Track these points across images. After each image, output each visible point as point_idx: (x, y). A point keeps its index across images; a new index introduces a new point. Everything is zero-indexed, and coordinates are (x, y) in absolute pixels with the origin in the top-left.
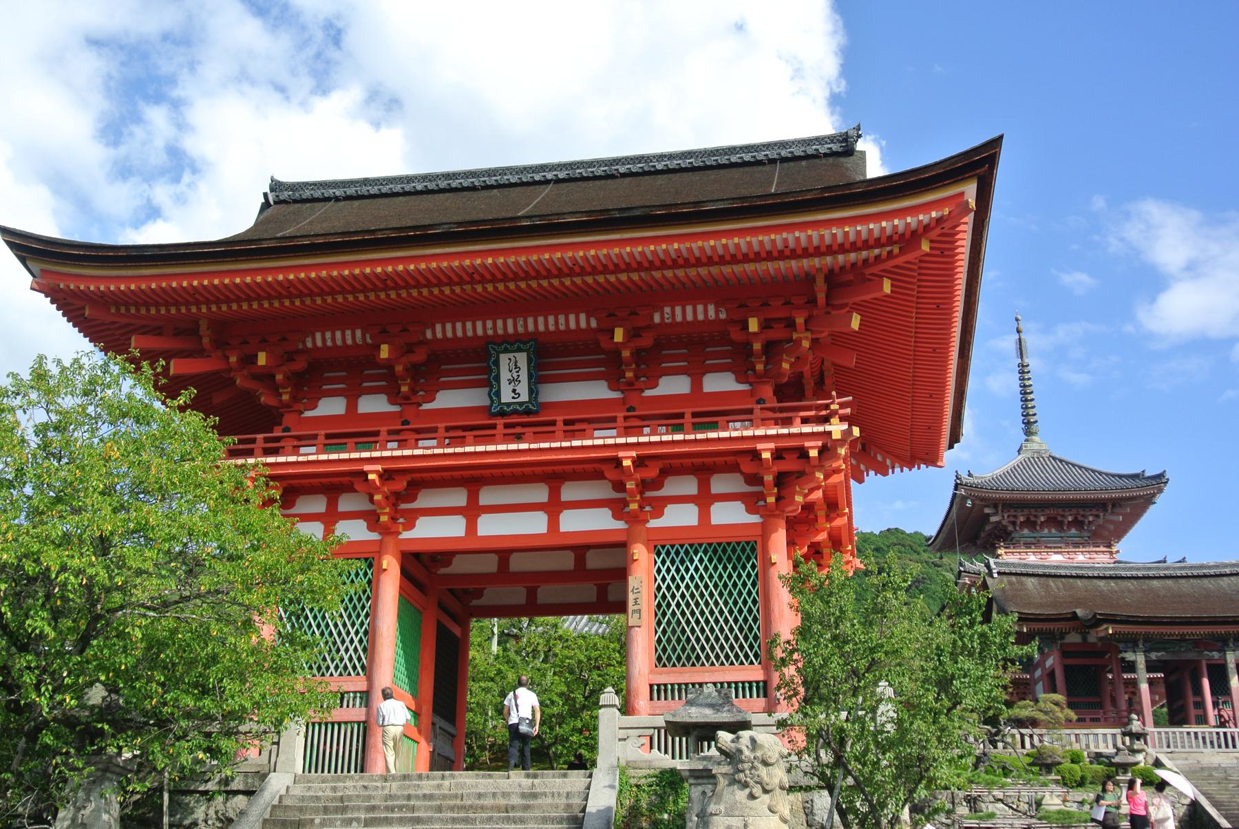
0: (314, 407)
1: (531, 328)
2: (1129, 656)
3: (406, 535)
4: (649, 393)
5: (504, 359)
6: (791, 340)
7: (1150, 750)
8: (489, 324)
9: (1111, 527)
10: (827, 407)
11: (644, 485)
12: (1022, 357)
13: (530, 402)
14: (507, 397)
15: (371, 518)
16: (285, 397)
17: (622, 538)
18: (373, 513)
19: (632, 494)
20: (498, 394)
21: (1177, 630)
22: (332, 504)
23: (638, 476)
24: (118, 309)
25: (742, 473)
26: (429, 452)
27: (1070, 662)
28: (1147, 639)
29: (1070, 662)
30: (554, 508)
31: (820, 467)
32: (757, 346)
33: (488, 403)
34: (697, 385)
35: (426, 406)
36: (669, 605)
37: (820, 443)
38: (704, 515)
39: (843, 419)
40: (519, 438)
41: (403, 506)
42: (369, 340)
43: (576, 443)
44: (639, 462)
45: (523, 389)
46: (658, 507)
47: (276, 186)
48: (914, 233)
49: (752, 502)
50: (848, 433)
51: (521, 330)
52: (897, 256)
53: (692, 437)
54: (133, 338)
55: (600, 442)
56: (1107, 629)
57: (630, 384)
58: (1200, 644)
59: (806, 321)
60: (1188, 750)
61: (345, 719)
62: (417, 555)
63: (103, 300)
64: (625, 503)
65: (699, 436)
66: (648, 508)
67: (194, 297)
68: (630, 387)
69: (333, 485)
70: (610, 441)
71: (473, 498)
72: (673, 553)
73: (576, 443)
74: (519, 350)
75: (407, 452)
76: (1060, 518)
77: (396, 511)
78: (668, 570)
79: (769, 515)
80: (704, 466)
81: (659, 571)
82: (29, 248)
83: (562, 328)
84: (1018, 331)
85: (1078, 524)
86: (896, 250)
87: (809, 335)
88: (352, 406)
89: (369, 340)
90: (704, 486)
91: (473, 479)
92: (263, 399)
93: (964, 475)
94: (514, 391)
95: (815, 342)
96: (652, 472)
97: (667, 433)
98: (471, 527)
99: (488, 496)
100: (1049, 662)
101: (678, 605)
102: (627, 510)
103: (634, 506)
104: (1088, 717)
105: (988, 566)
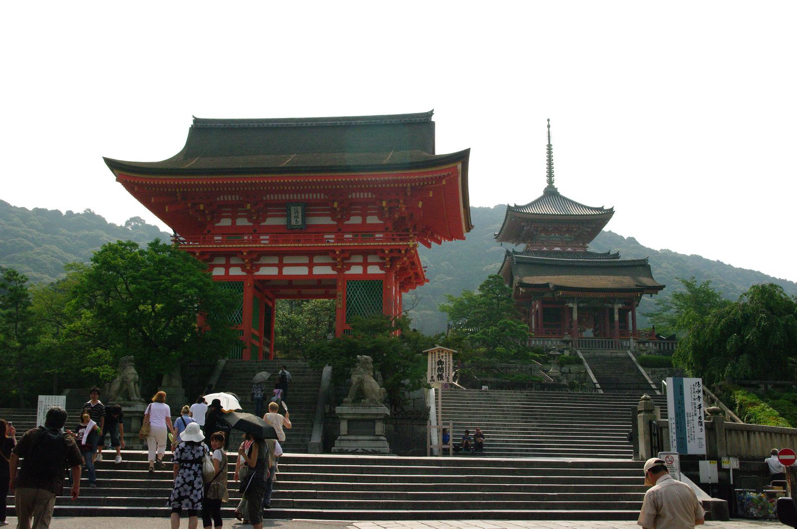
0: (219, 222)
2: (570, 305)
3: (256, 273)
4: (346, 222)
5: (293, 208)
6: (398, 207)
9: (586, 233)
10: (408, 235)
12: (549, 142)
14: (293, 222)
16: (209, 219)
19: (339, 262)
20: (290, 221)
21: (591, 295)
22: (228, 261)
23: (341, 256)
24: (148, 188)
30: (311, 265)
31: (405, 256)
32: (386, 209)
33: (286, 223)
34: (364, 220)
36: (351, 302)
37: (405, 248)
38: (365, 270)
40: (299, 241)
43: (320, 245)
44: (342, 252)
45: (300, 220)
47: (196, 121)
52: (434, 184)
56: (560, 293)
60: (591, 348)
62: (259, 281)
67: (178, 186)
72: (353, 283)
74: (299, 205)
75: (258, 245)
76: (560, 229)
77: (252, 264)
79: (388, 271)
80: (365, 253)
81: (348, 290)
84: (549, 126)
85: (569, 231)
86: (434, 182)
87: (404, 206)
88: (234, 223)
89: (241, 199)
90: (365, 259)
91: (281, 254)
92: (199, 219)
93: (513, 206)
95: (407, 208)
98: (280, 271)
99: (286, 260)
100: (537, 306)
101: (355, 302)
103: (340, 267)
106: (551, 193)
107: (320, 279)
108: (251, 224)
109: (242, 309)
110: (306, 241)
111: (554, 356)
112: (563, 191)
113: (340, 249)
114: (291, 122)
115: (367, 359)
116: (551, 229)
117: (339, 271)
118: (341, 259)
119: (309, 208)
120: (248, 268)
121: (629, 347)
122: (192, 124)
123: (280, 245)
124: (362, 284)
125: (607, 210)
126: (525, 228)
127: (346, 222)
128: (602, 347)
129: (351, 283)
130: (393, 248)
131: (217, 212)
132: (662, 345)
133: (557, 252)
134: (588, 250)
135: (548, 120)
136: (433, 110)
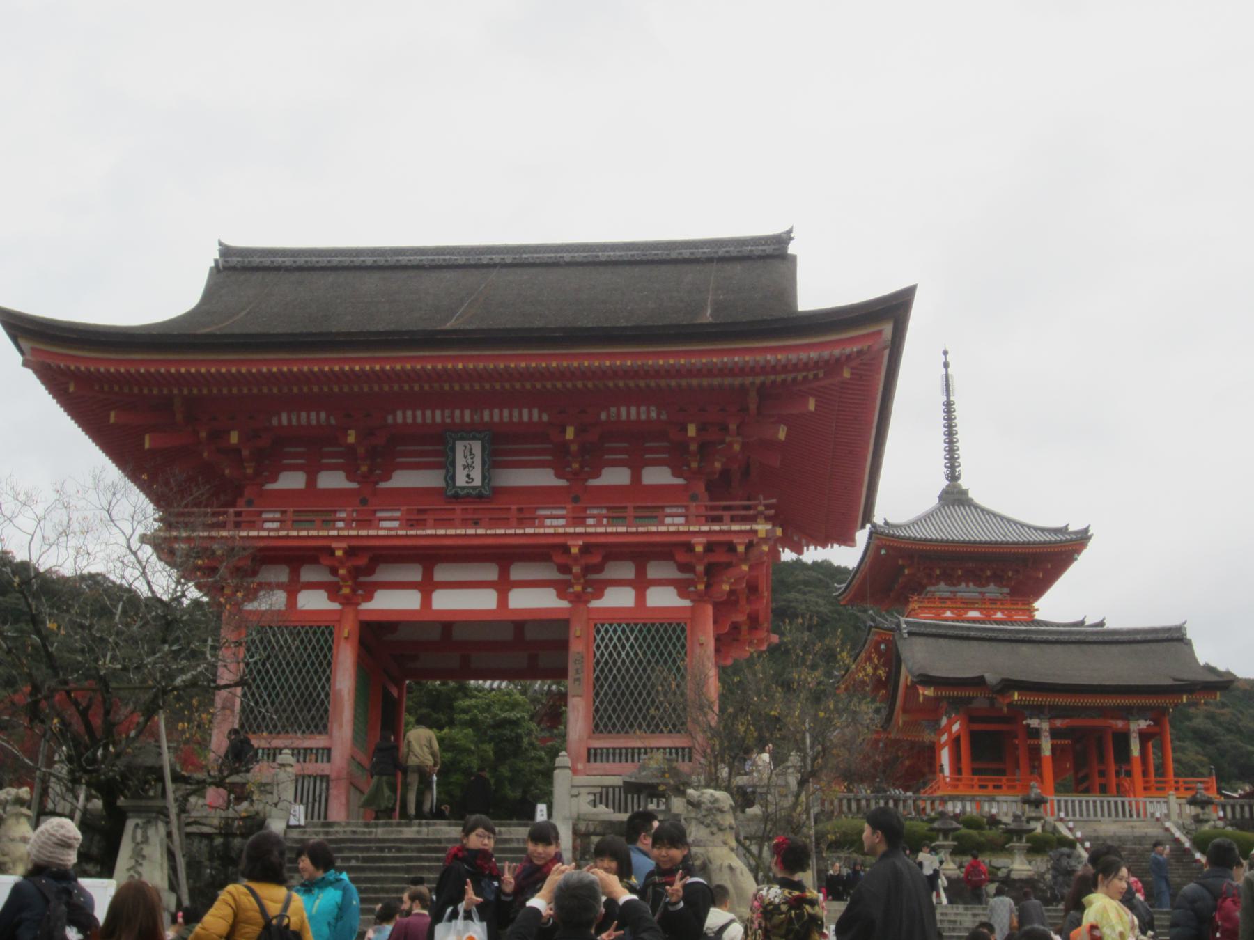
1: (486, 418)
2: (1034, 723)
3: (365, 606)
4: (593, 482)
5: (460, 447)
6: (722, 442)
7: (1050, 819)
8: (447, 413)
11: (587, 569)
12: (948, 395)
13: (483, 486)
14: (461, 480)
15: (333, 591)
16: (250, 471)
17: (566, 617)
18: (337, 583)
19: (576, 577)
20: (453, 478)
23: (583, 562)
25: (676, 562)
26: (393, 533)
27: (976, 727)
28: (1053, 708)
29: (976, 727)
30: (503, 586)
32: (693, 447)
34: (636, 477)
35: (383, 485)
36: (606, 678)
38: (641, 598)
39: (768, 519)
40: (476, 523)
41: (362, 579)
42: (333, 422)
44: (586, 549)
46: (599, 589)
47: (226, 251)
48: (838, 360)
49: (682, 588)
50: (773, 531)
51: (476, 418)
53: (634, 530)
54: (113, 414)
55: (551, 531)
57: (576, 474)
58: (1105, 712)
59: (738, 427)
61: (320, 772)
63: (85, 379)
64: (568, 584)
65: (641, 529)
66: (589, 590)
67: (179, 380)
68: (577, 477)
69: (295, 558)
70: (561, 530)
71: (428, 573)
73: (530, 531)
74: (474, 438)
75: (372, 532)
78: (606, 647)
79: (699, 599)
81: (598, 647)
82: (26, 330)
83: (515, 419)
84: (946, 365)
85: (998, 579)
86: (821, 375)
87: (740, 439)
88: (311, 481)
89: (333, 422)
90: (641, 571)
91: (429, 558)
92: (227, 472)
94: (468, 476)
95: (744, 446)
96: (595, 559)
97: (608, 525)
98: (426, 601)
100: (956, 727)
101: (615, 678)
102: (571, 590)
103: (578, 588)
104: (990, 784)
105: (898, 625)
106: (954, 497)
107: (521, 625)
108: (354, 485)
109: (327, 695)
110: (496, 522)
111: (1019, 833)
112: (976, 495)
113: (581, 543)
114: (453, 254)
115: (716, 800)
116: (960, 572)
117: (579, 600)
118: (582, 568)
119: (502, 447)
120: (346, 591)
121: (1168, 816)
122: (217, 256)
123: (429, 532)
124: (632, 631)
125: (1075, 533)
126: (906, 572)
127: (593, 482)
128: (1110, 815)
129: (607, 631)
130: (714, 538)
131: (272, 456)
132: (1238, 809)
133: (974, 620)
134: (1038, 616)
135: (945, 353)
136: (790, 231)
